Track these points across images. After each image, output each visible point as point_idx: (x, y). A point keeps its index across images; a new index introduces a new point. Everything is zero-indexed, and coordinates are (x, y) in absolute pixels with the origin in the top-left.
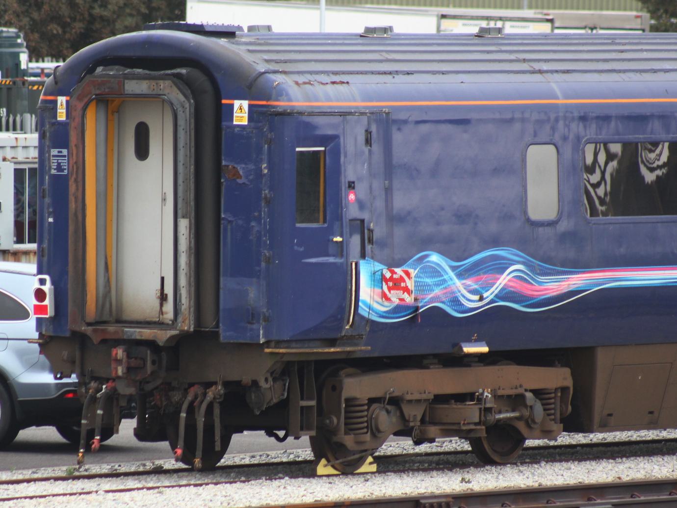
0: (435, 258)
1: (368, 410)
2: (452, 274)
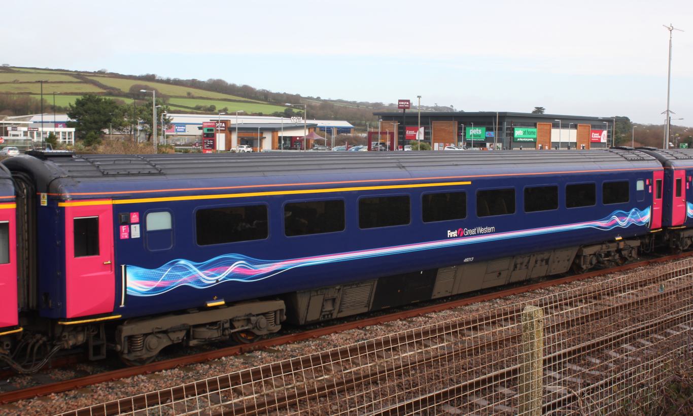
0: (183, 262)
1: (144, 341)
2: (195, 269)
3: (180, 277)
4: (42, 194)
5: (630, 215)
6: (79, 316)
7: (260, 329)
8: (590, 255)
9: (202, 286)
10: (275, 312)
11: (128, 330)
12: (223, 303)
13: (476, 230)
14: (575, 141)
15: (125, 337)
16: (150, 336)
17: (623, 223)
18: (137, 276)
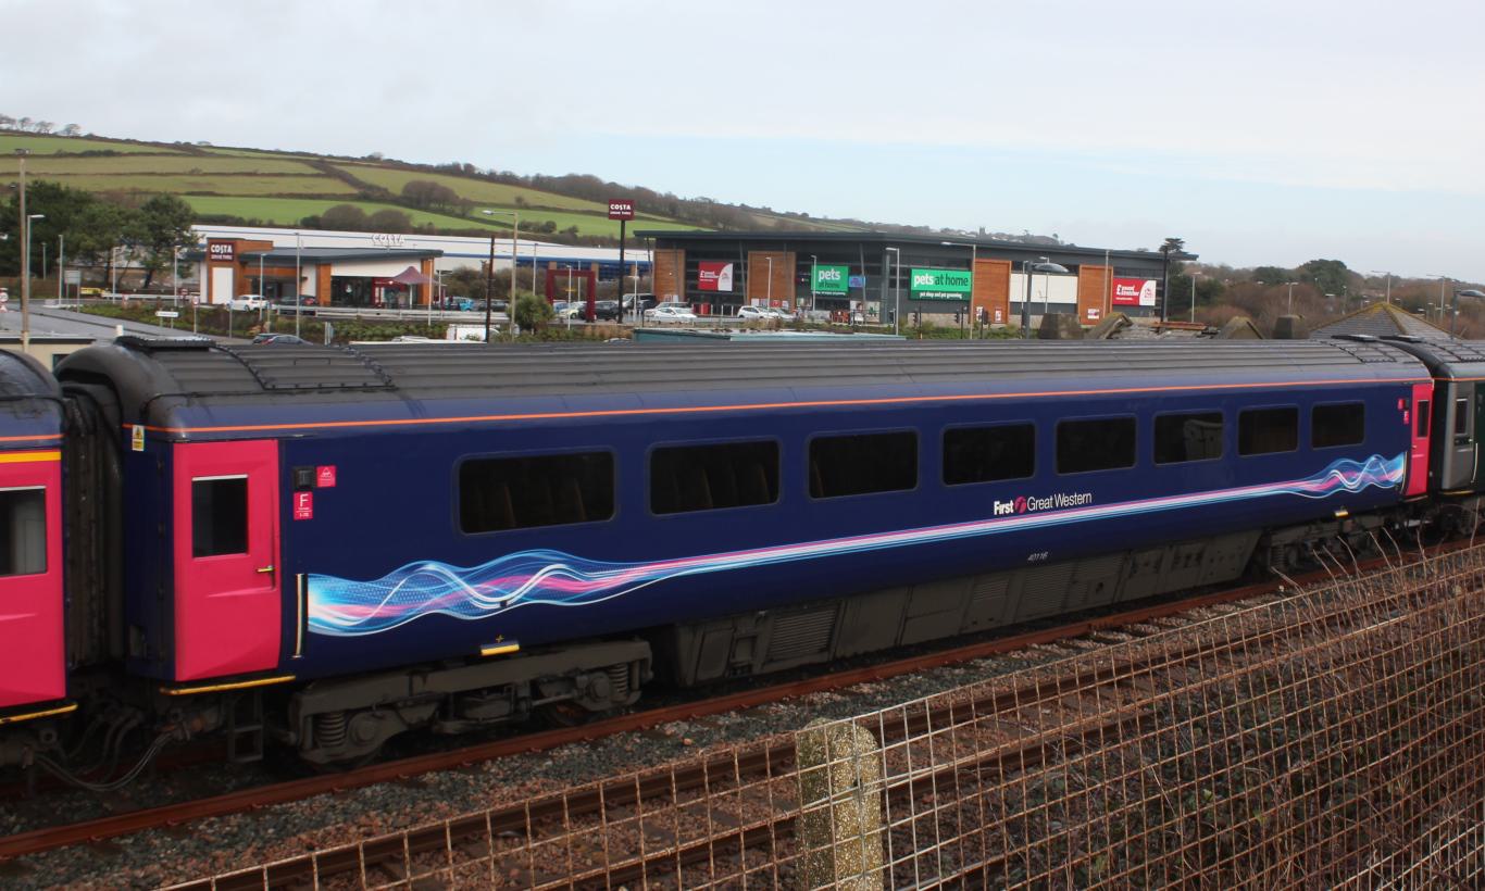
1: (347, 725)
2: (458, 580)
3: (425, 597)
4: (135, 428)
5: (1365, 469)
6: (199, 678)
7: (595, 698)
8: (1286, 546)
9: (477, 615)
10: (630, 665)
11: (313, 702)
12: (515, 647)
13: (1054, 501)
14: (1073, 300)
15: (306, 717)
16: (361, 715)
17: (1352, 483)
18: (334, 596)
